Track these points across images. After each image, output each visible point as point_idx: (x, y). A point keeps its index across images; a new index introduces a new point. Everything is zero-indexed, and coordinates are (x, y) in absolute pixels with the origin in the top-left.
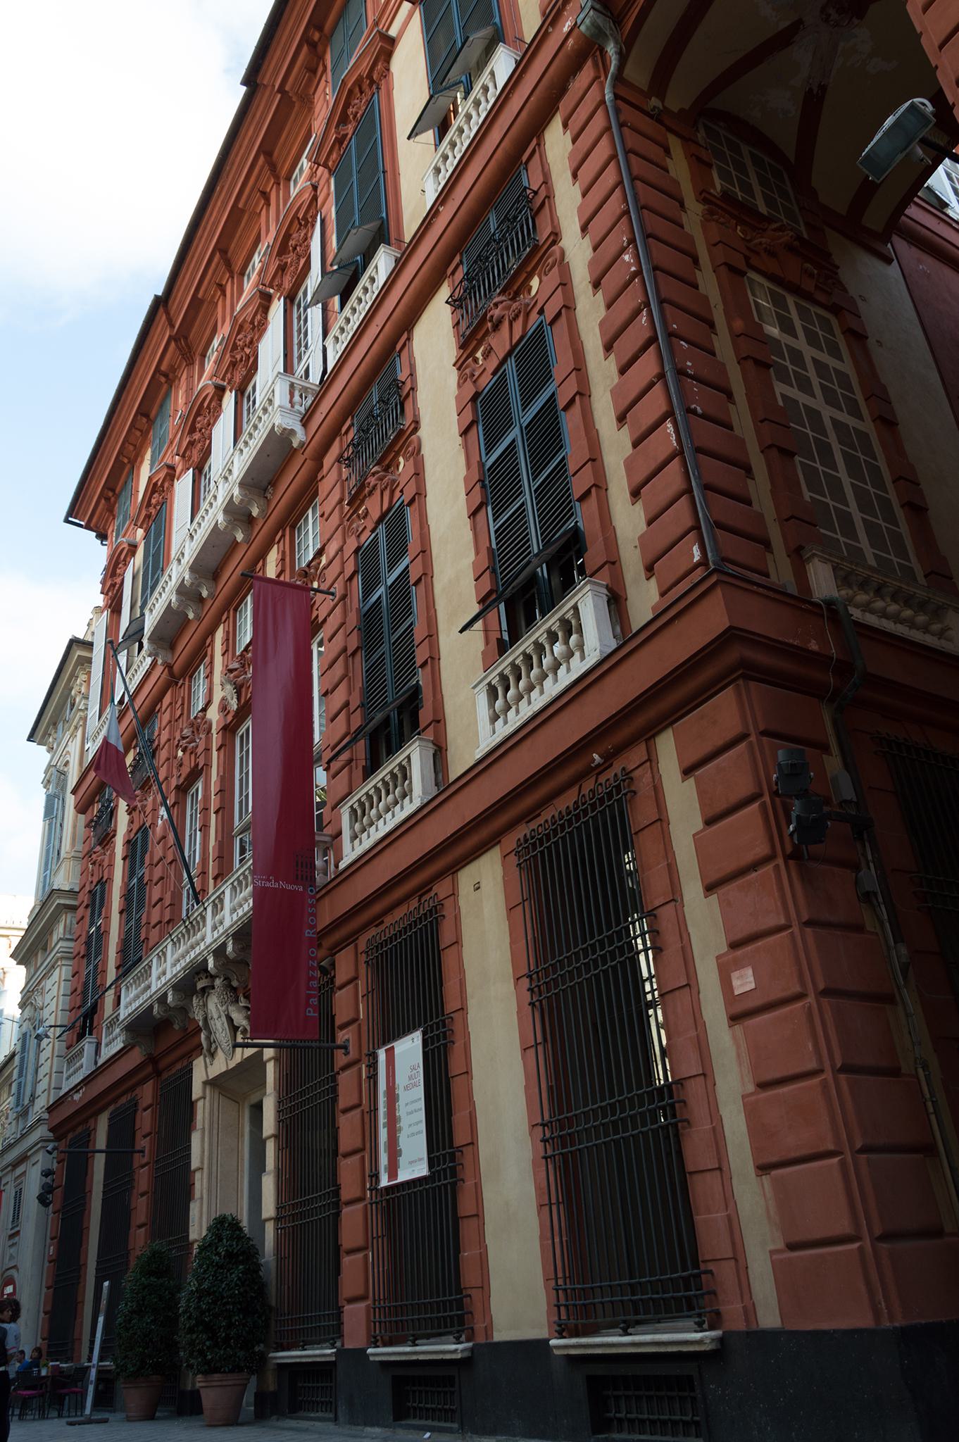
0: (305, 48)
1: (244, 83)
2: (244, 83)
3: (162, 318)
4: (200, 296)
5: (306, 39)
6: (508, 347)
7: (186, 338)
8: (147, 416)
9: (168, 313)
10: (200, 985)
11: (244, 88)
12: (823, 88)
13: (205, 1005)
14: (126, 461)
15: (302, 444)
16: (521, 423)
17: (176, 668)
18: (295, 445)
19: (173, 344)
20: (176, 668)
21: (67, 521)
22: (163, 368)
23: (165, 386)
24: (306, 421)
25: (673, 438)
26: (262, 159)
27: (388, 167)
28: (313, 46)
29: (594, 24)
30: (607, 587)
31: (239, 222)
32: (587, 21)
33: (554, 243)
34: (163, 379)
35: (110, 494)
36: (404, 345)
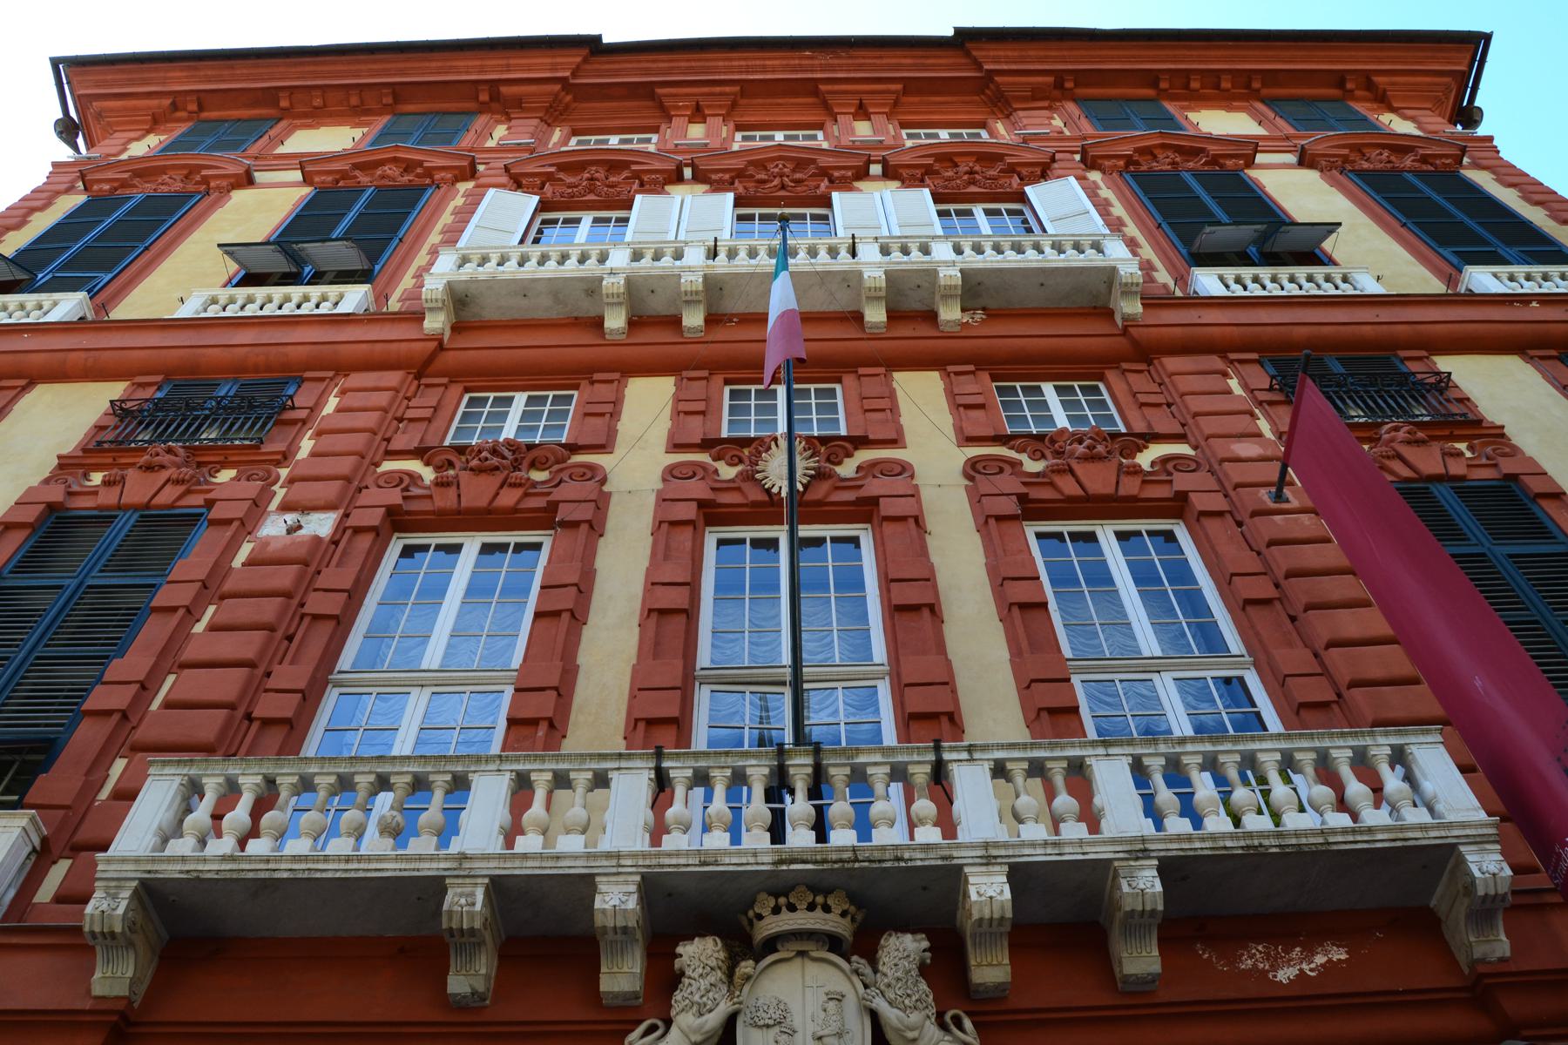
0: (1051, 79)
2: (958, 31)
3: (575, 58)
4: (659, 91)
5: (1060, 76)
7: (575, 100)
8: (397, 99)
9: (585, 61)
11: (950, 33)
14: (284, 103)
17: (448, 359)
19: (557, 87)
20: (448, 359)
22: (504, 89)
23: (471, 105)
26: (899, 87)
27: (1403, 231)
28: (1058, 84)
31: (796, 94)
34: (484, 97)
35: (193, 107)
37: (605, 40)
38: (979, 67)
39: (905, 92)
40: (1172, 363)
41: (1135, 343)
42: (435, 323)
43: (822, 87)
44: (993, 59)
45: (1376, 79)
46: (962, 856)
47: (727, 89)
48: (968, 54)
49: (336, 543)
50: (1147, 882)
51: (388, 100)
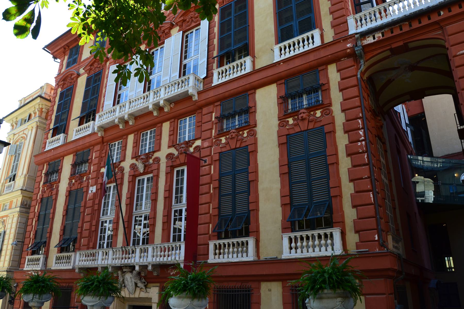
6: (306, 129)
10: (124, 270)
12: (394, 80)
13: (124, 275)
15: (196, 101)
16: (305, 153)
17: (105, 139)
18: (194, 100)
21: (44, 49)
24: (199, 93)
25: (372, 199)
29: (361, 53)
30: (341, 230)
32: (359, 52)
33: (329, 106)
35: (67, 47)
36: (252, 93)
40: (205, 110)
46: (135, 264)
49: (96, 192)
50: (150, 268)
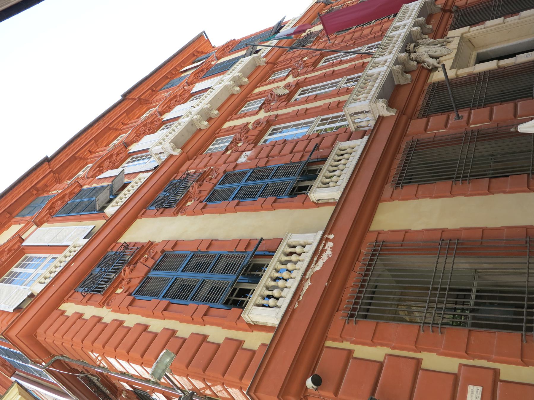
0: (150, 91)
1: (122, 96)
3: (46, 165)
11: (121, 98)
22: (38, 186)
26: (125, 114)
28: (153, 91)
31: (106, 133)
34: (35, 192)
37: (49, 157)
38: (135, 99)
39: (127, 115)
41: (271, 63)
42: (177, 152)
43: (111, 126)
44: (136, 95)
45: (198, 50)
47: (92, 143)
48: (129, 99)
51: (8, 215)
